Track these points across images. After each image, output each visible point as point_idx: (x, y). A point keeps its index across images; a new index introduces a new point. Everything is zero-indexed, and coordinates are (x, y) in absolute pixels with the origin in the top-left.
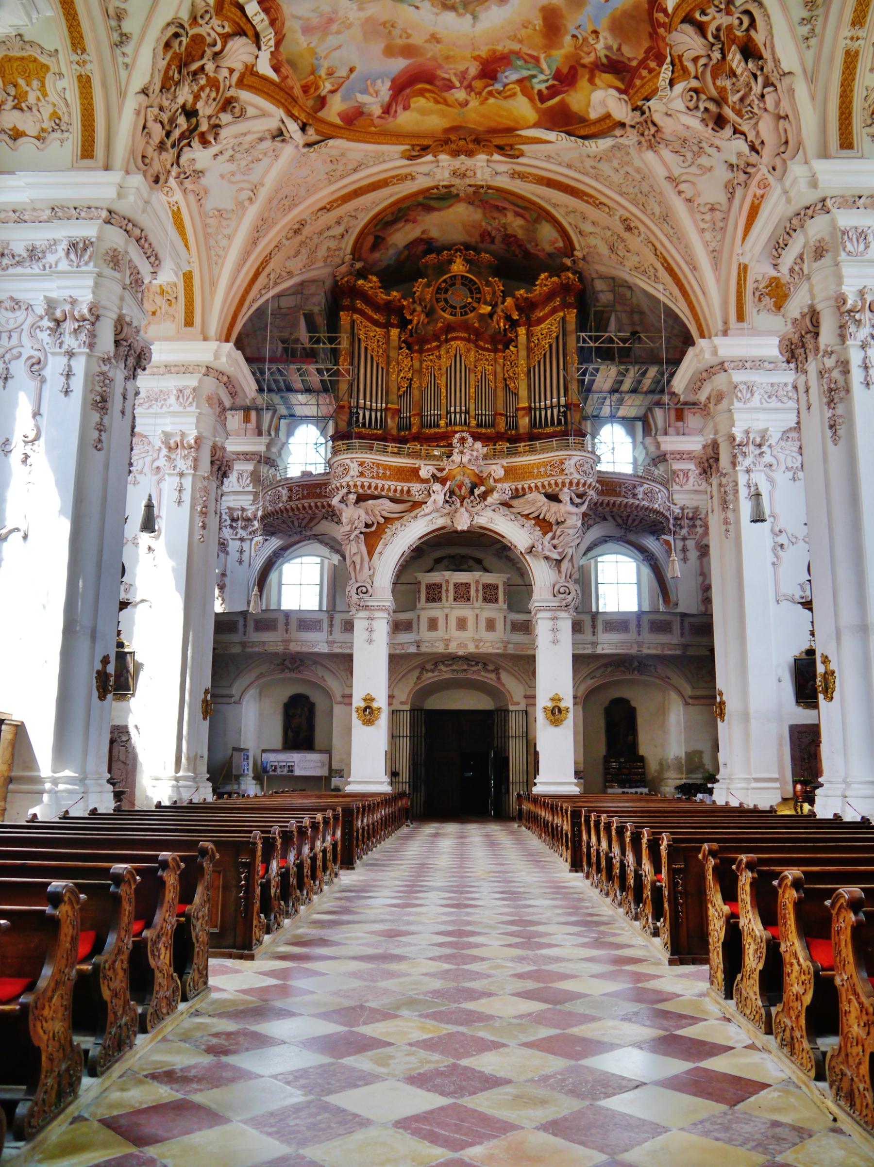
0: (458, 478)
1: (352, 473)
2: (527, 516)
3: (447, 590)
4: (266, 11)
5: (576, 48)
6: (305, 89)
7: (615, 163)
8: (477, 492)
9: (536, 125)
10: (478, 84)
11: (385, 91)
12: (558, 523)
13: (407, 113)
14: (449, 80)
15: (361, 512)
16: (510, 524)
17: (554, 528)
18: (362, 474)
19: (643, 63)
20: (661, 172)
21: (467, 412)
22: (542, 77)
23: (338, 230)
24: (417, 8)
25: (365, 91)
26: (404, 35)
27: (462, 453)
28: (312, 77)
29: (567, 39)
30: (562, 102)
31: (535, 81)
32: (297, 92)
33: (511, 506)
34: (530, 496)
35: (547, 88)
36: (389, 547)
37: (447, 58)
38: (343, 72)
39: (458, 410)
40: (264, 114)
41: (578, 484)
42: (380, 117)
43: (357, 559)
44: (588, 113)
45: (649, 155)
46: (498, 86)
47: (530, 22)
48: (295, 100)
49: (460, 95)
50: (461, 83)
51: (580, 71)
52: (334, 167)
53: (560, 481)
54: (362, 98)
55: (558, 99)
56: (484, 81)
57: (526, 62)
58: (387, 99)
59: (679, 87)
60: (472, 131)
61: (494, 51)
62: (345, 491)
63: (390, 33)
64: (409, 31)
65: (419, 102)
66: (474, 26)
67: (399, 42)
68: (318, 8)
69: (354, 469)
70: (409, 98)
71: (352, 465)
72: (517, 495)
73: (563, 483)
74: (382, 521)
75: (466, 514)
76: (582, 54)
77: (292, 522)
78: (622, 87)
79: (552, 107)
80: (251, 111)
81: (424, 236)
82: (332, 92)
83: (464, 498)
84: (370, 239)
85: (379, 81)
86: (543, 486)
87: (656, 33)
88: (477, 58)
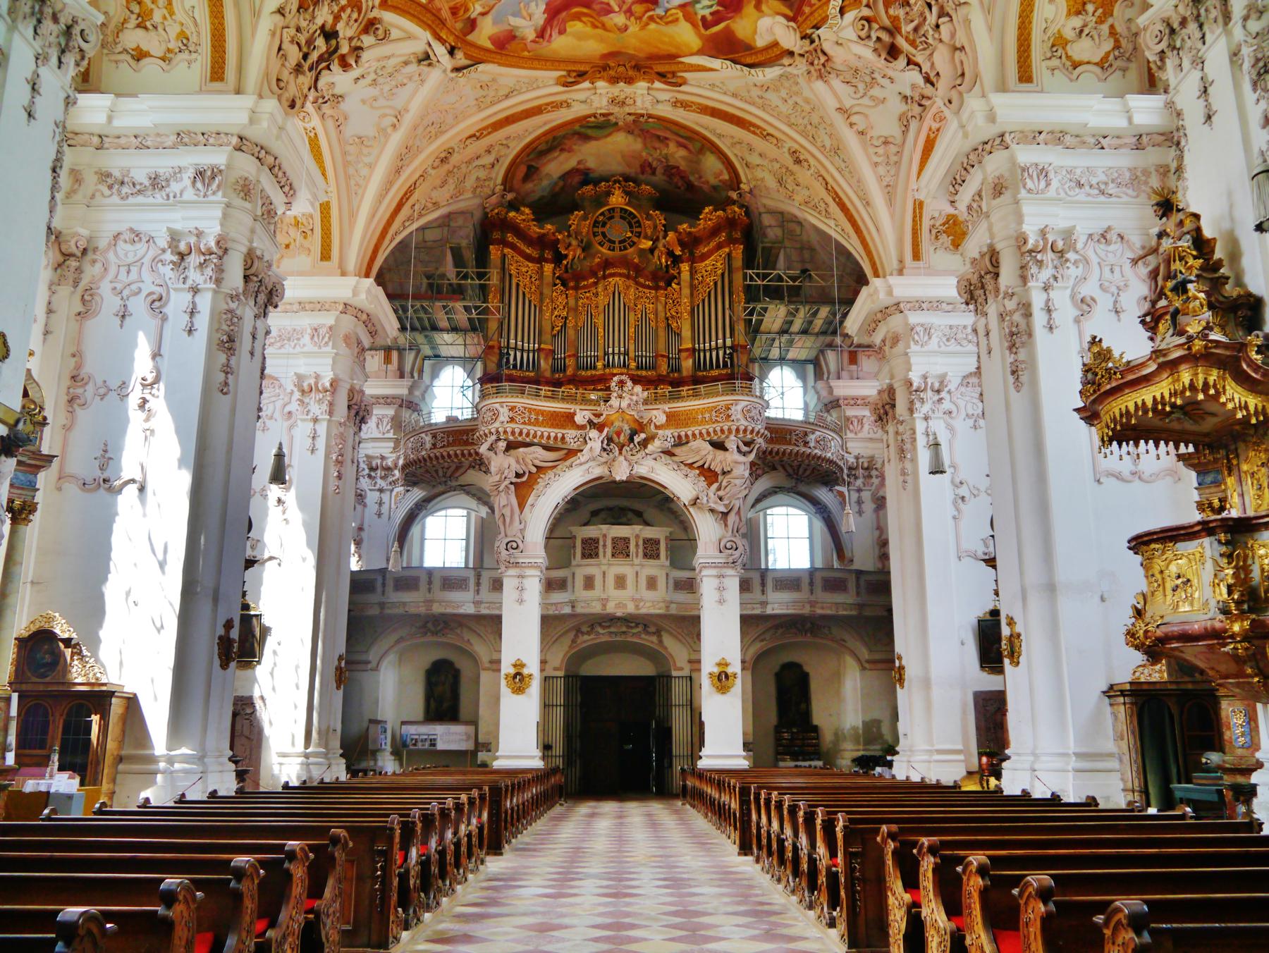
0: (617, 424)
1: (501, 418)
2: (690, 466)
3: (605, 546)
6: (454, 11)
7: (783, 93)
8: (637, 439)
9: (700, 52)
11: (539, 17)
12: (724, 473)
13: (563, 37)
14: (608, 4)
15: (512, 461)
16: (673, 473)
17: (720, 478)
18: (512, 420)
20: (831, 103)
21: (626, 353)
23: (487, 160)
27: (621, 397)
30: (727, 28)
32: (445, 14)
33: (674, 455)
34: (694, 444)
35: (712, 14)
36: (542, 499)
39: (616, 350)
40: (410, 37)
41: (745, 431)
42: (533, 41)
43: (507, 512)
45: (819, 85)
46: (660, 11)
48: (443, 23)
49: (619, 19)
50: (620, 8)
52: (484, 93)
53: (726, 428)
54: (515, 21)
55: (722, 25)
58: (541, 22)
59: (850, 16)
60: (631, 57)
62: (494, 437)
65: (575, 27)
69: (504, 414)
70: (564, 22)
71: (501, 410)
72: (680, 442)
73: (730, 430)
74: (534, 470)
75: (625, 463)
77: (437, 471)
78: (791, 14)
79: (716, 34)
80: (395, 34)
81: (581, 167)
82: (483, 14)
83: (623, 446)
84: (522, 170)
85: (533, 4)
86: (708, 433)
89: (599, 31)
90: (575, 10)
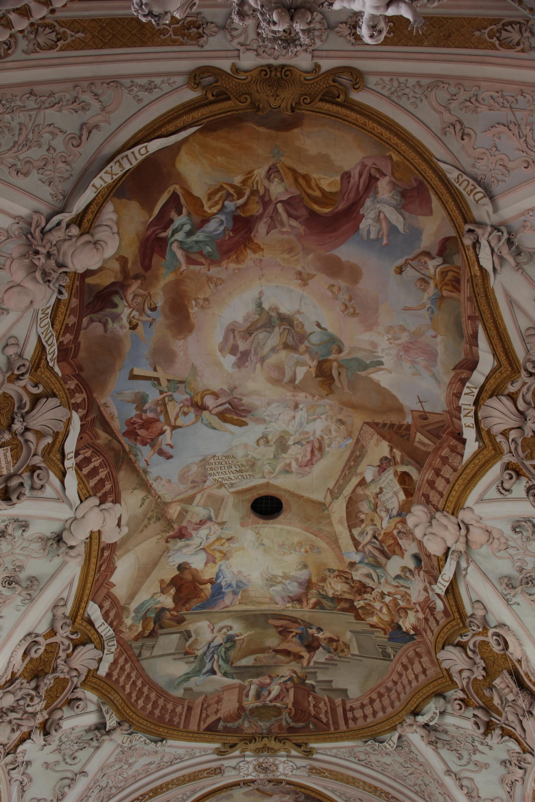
4: (459, 409)
5: (149, 294)
9: (176, 148)
10: (255, 209)
13: (346, 169)
14: (290, 215)
19: (76, 329)
22: (180, 236)
24: (318, 325)
25: (393, 229)
26: (335, 289)
28: (445, 293)
29: (160, 301)
30: (150, 210)
31: (187, 228)
32: (466, 290)
35: (172, 221)
37: (290, 250)
38: (409, 272)
40: (511, 302)
42: (384, 175)
44: (116, 211)
46: (230, 205)
47: (202, 307)
49: (278, 190)
50: (276, 209)
51: (139, 269)
54: (396, 218)
56: (249, 214)
57: (201, 253)
58: (368, 202)
61: (238, 261)
63: (350, 300)
64: (330, 294)
65: (329, 182)
66: (261, 293)
67: (342, 283)
68: (414, 374)
70: (341, 193)
76: (142, 292)
78: (89, 281)
80: (524, 324)
82: (427, 254)
85: (373, 236)
87: (78, 377)
88: (257, 249)
89: (302, 170)
90: (326, 210)
